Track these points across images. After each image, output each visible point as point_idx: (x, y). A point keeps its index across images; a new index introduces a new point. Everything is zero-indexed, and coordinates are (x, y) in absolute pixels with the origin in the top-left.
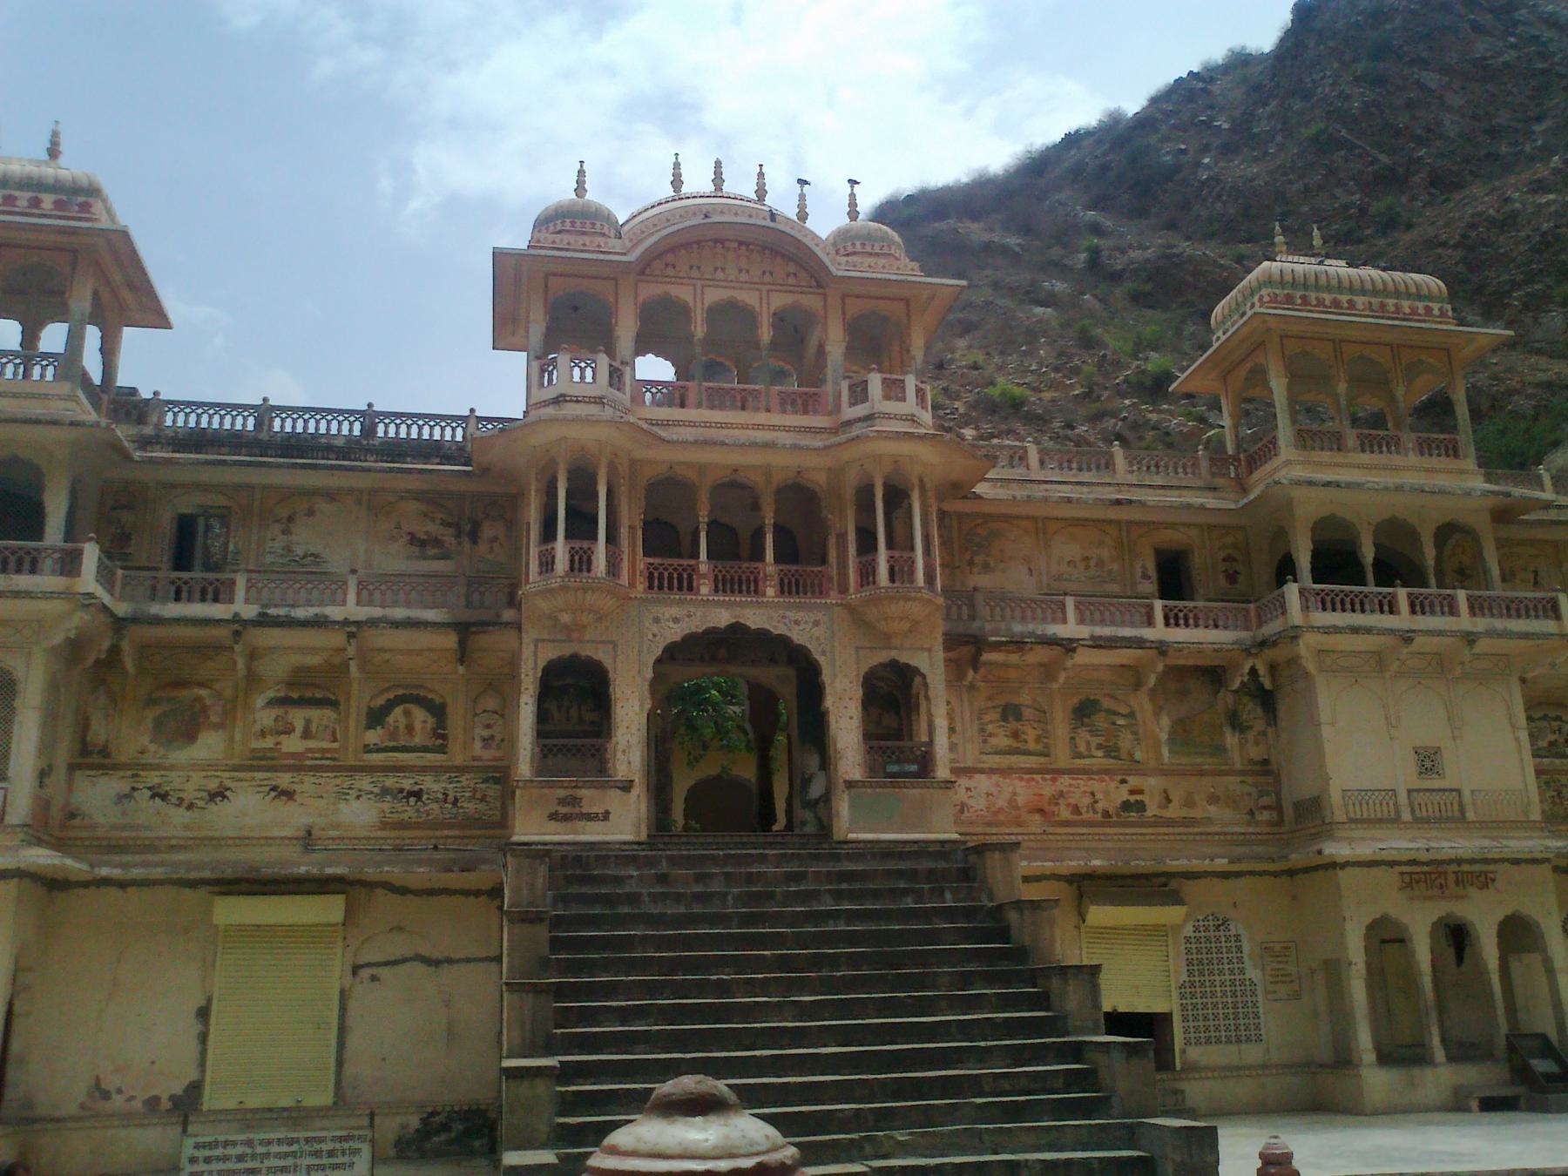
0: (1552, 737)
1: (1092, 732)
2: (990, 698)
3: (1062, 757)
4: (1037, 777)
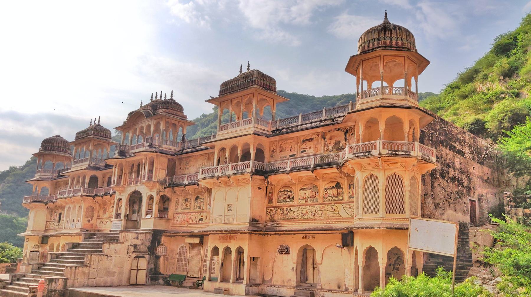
0: (284, 196)
1: (198, 203)
2: (184, 197)
3: (192, 210)
4: (188, 214)
